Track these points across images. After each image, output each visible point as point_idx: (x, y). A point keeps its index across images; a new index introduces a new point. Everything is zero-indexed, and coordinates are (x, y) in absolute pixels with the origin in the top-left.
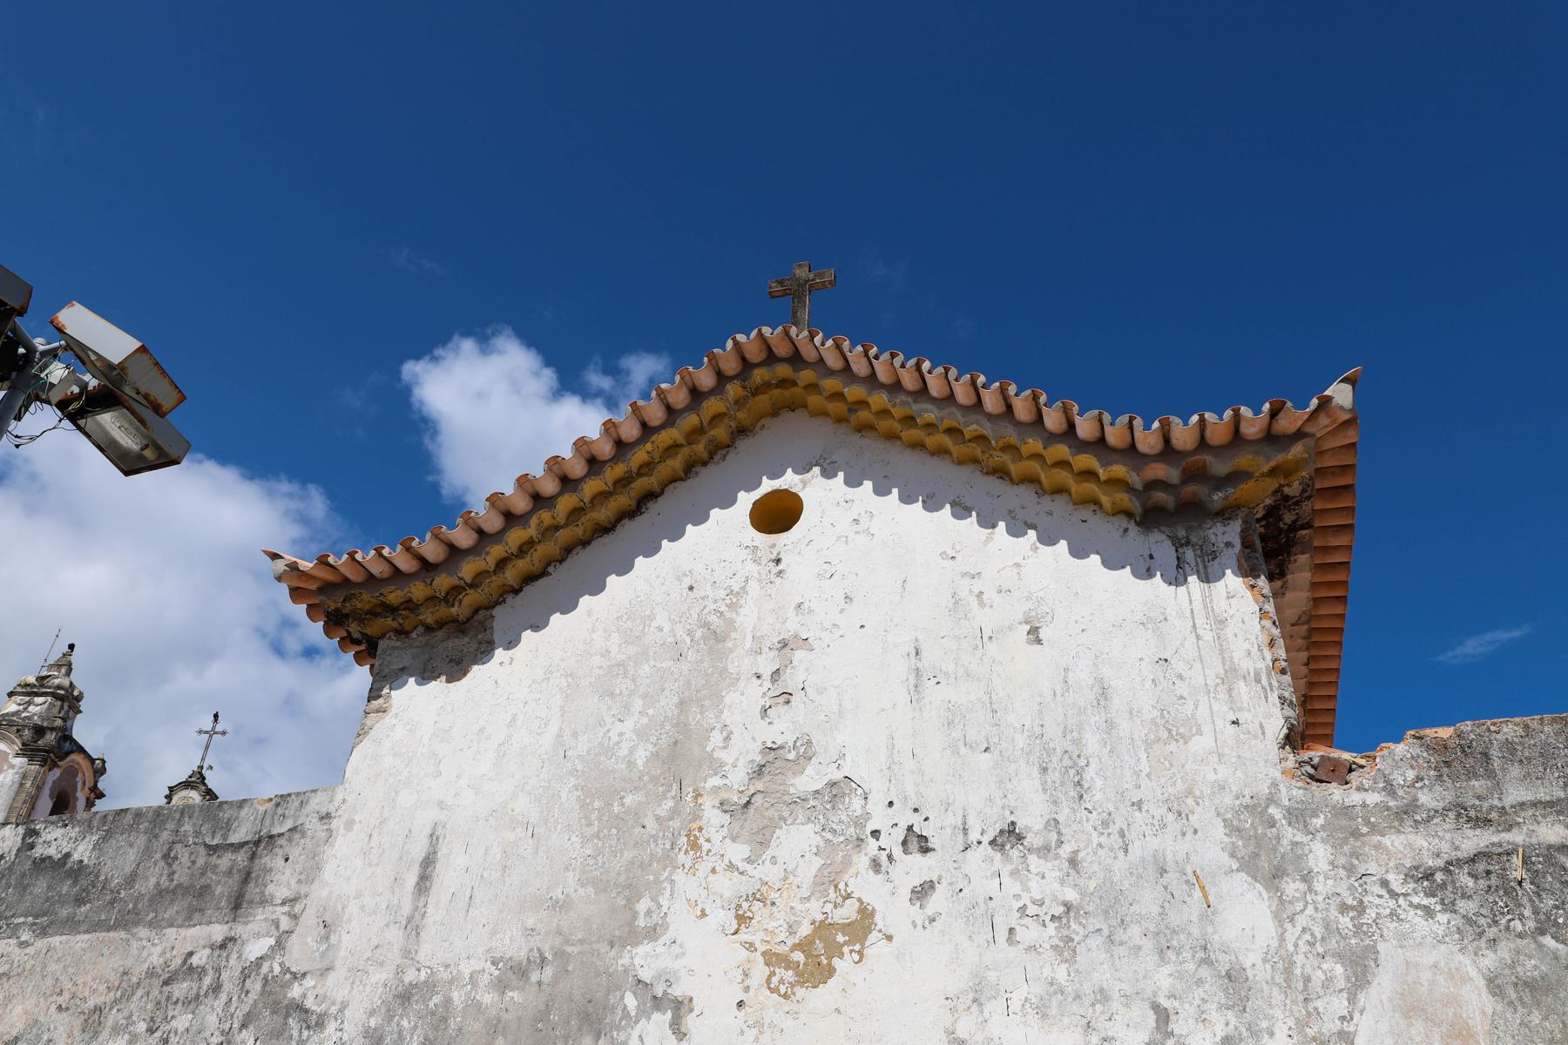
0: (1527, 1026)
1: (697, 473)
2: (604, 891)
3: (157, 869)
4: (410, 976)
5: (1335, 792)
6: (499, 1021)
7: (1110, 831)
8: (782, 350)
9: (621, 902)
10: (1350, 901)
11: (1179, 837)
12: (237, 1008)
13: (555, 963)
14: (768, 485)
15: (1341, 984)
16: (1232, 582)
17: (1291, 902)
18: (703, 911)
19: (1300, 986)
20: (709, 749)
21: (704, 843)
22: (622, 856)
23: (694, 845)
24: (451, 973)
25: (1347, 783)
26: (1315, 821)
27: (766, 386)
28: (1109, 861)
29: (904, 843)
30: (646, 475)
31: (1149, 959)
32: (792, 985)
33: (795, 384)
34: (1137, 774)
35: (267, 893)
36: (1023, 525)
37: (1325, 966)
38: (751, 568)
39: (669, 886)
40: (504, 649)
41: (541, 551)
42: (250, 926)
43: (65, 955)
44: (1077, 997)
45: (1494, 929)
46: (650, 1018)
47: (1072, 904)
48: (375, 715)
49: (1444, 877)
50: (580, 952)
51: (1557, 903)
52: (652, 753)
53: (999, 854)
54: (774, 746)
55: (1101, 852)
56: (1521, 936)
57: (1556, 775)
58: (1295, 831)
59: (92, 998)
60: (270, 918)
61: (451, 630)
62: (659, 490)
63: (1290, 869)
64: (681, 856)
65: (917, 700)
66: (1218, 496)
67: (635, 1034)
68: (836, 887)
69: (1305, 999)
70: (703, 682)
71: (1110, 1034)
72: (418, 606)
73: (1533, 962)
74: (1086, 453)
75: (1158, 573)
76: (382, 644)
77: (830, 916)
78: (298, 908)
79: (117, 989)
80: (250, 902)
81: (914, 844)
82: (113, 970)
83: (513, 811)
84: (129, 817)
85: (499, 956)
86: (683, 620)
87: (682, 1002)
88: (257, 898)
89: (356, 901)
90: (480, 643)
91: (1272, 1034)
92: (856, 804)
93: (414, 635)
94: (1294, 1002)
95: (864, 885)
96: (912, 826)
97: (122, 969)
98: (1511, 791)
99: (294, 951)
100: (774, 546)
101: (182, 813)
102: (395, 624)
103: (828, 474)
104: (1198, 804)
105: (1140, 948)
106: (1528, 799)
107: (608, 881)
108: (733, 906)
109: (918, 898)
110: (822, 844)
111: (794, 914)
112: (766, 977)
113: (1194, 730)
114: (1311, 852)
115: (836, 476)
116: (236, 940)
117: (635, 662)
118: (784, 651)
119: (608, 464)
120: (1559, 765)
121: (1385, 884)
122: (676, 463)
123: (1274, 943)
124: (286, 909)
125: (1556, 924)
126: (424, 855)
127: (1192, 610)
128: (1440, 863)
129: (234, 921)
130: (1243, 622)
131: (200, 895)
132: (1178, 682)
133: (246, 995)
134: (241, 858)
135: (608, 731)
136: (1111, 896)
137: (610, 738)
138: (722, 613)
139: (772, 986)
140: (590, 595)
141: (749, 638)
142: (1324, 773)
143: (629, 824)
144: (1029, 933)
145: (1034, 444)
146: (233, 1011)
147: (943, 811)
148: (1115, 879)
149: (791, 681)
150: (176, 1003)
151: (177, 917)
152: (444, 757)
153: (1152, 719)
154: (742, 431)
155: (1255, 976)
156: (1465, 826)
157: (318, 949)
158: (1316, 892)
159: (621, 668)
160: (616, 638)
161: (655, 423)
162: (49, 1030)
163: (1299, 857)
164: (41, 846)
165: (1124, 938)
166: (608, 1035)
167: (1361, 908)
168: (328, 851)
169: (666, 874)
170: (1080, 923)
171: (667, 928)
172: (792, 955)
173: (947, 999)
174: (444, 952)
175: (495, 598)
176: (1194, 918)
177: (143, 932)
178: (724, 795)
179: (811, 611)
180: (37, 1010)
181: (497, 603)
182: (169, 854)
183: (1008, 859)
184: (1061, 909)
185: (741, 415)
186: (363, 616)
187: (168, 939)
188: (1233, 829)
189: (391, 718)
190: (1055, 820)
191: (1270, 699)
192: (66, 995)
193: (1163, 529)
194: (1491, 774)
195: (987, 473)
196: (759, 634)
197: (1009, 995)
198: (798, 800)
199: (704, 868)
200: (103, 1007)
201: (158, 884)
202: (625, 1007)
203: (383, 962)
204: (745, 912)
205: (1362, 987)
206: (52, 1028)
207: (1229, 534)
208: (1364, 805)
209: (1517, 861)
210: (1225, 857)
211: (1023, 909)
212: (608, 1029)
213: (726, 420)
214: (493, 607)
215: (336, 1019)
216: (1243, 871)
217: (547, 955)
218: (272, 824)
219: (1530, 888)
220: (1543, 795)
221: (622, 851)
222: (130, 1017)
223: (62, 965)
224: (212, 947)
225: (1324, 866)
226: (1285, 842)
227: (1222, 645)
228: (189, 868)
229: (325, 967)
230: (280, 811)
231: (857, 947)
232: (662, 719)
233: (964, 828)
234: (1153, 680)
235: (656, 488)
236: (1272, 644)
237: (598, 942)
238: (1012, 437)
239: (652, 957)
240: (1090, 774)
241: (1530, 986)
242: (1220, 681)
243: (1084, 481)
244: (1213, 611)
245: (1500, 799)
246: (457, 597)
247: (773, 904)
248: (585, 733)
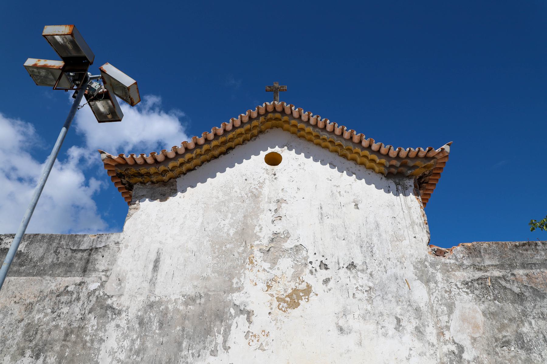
0: (492, 325)
1: (246, 143)
2: (221, 275)
3: (52, 256)
4: (152, 299)
5: (443, 259)
6: (186, 315)
7: (381, 266)
8: (279, 109)
9: (227, 279)
10: (447, 290)
11: (401, 269)
12: (87, 306)
13: (205, 297)
14: (270, 150)
15: (446, 312)
16: (412, 197)
17: (432, 289)
18: (256, 283)
19: (435, 313)
20: (255, 232)
21: (255, 262)
22: (227, 264)
23: (251, 262)
24: (167, 299)
25: (444, 257)
26: (438, 267)
27: (271, 119)
28: (381, 275)
29: (320, 266)
31: (394, 304)
32: (286, 308)
33: (280, 120)
34: (388, 250)
35: (96, 268)
36: (352, 173)
37: (442, 307)
38: (266, 176)
39: (243, 274)
40: (181, 193)
41: (195, 162)
42: (90, 278)
43: (16, 284)
44: (374, 314)
45: (484, 299)
46: (239, 317)
47: (371, 287)
48: (134, 210)
49: (471, 284)
50: (213, 294)
52: (235, 232)
53: (349, 271)
54: (277, 233)
55: (379, 272)
56: (490, 300)
57: (497, 258)
58: (432, 269)
59: (28, 299)
60: (98, 276)
61: (161, 184)
62: (234, 147)
63: (431, 280)
64: (247, 266)
65: (322, 222)
66: (409, 172)
67: (235, 321)
68: (299, 278)
69: (437, 316)
70: (252, 210)
71: (384, 325)
72: (151, 175)
73: (493, 308)
75: (391, 192)
76: (135, 186)
77: (298, 287)
78: (108, 273)
79: (38, 297)
80: (90, 270)
81: (323, 267)
82: (36, 290)
83: (187, 246)
84: (40, 237)
85: (185, 294)
86: (244, 190)
87: (250, 312)
88: (92, 269)
89: (131, 272)
90: (172, 189)
91: (428, 326)
92: (304, 253)
93: (147, 184)
94: (434, 317)
95: (308, 278)
96: (322, 261)
97: (40, 290)
98: (486, 261)
99: (108, 288)
100: (273, 170)
101: (61, 237)
102: (141, 180)
103: (290, 149)
104: (406, 260)
105: (391, 301)
107: (222, 272)
108: (266, 282)
109: (325, 283)
110: (294, 265)
111: (286, 286)
112: (278, 305)
113: (404, 239)
114: (437, 275)
115: (292, 150)
116: (85, 283)
117: (228, 201)
118: (278, 203)
121: (456, 285)
122: (241, 139)
123: (428, 301)
124: (104, 273)
125: (498, 298)
126: (155, 259)
128: (470, 280)
129: (84, 276)
130: (416, 209)
131: (70, 266)
132: (398, 224)
133: (90, 302)
134: (85, 255)
135: (220, 223)
136: (382, 285)
137: (220, 225)
138: (257, 189)
139: (280, 308)
140: (211, 178)
141: (267, 198)
142: (438, 253)
143: (229, 254)
144: (359, 295)
145: (358, 150)
146: (85, 307)
147: (331, 257)
148: (384, 280)
149: (281, 212)
150: (63, 303)
151: (61, 273)
152: (161, 227)
153: (392, 234)
154: (261, 132)
155: (423, 310)
157: (117, 288)
158: (438, 287)
159: (223, 203)
160: (221, 193)
162: (11, 310)
163: (434, 277)
164: (3, 244)
165: (387, 298)
166: (225, 321)
167: (450, 292)
168: (119, 255)
169: (242, 271)
170: (374, 293)
171: (244, 288)
172: (286, 298)
173: (336, 314)
174: (164, 291)
175: (177, 175)
176: (406, 293)
177: (48, 278)
178: (261, 247)
179: (286, 192)
180: (6, 303)
181: (178, 177)
182: (57, 251)
183: (351, 273)
184: (368, 289)
185: (263, 127)
186: (130, 176)
187: (58, 281)
188: (416, 268)
189: (140, 212)
190: (365, 262)
192: (18, 298)
193: (392, 179)
194: (481, 257)
195: (340, 156)
196: (269, 197)
197: (354, 313)
198: (285, 250)
199: (255, 270)
200: (33, 303)
201: (52, 261)
202: (231, 313)
203: (142, 293)
204: (270, 285)
205: (451, 313)
206: (12, 309)
207: (410, 183)
208: (450, 263)
209: (488, 280)
210: (414, 276)
211: (357, 288)
212: (225, 320)
213: (258, 128)
214: (176, 178)
215: (125, 312)
216: (419, 280)
217: (202, 294)
218: (97, 244)
220: (494, 263)
221: (226, 263)
222: (44, 307)
223: (15, 287)
224: (76, 285)
225: (440, 280)
226: (430, 272)
227: (410, 215)
228: (65, 257)
229: (120, 294)
230: (99, 240)
231: (307, 297)
232: (238, 221)
233: (338, 263)
234: (392, 223)
235: (233, 146)
236: (423, 216)
237: (220, 291)
238: (351, 147)
239: (239, 297)
240: (375, 249)
241: (492, 314)
242: (410, 225)
243: (371, 162)
244: (407, 204)
245: (484, 263)
246: (165, 173)
247: (279, 282)
248: (211, 223)
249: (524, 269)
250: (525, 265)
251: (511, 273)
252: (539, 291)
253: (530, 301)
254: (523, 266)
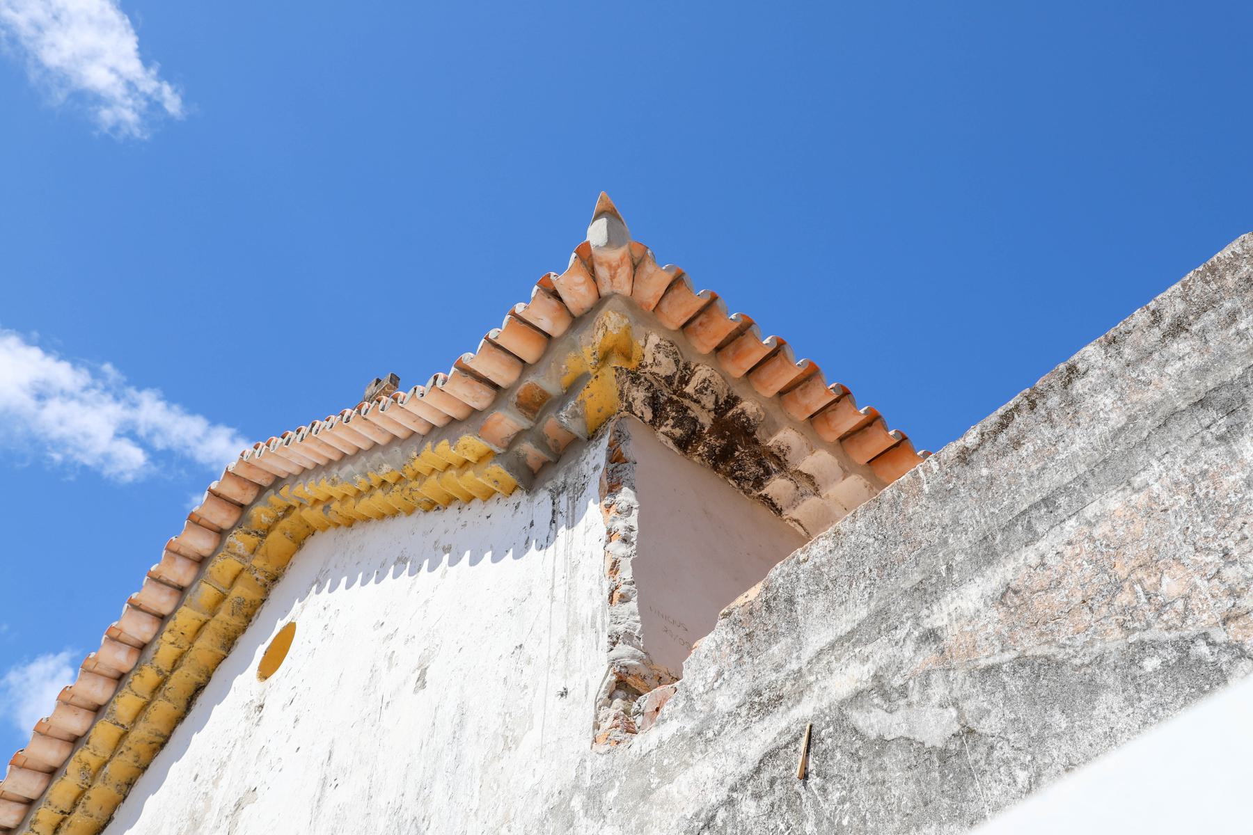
30: (179, 667)
41: (100, 794)
51: (844, 793)
57: (862, 586)
74: (442, 440)
106: (828, 640)
119: (133, 673)
120: (867, 571)
122: (206, 645)
127: (554, 568)
128: (723, 793)
156: (754, 719)
161: (166, 610)
191: (600, 645)
194: (793, 624)
219: (815, 784)
220: (844, 627)
236: (614, 568)
249: (990, 563)
250: (999, 537)
251: (916, 633)
252: (1060, 665)
253: (1006, 762)
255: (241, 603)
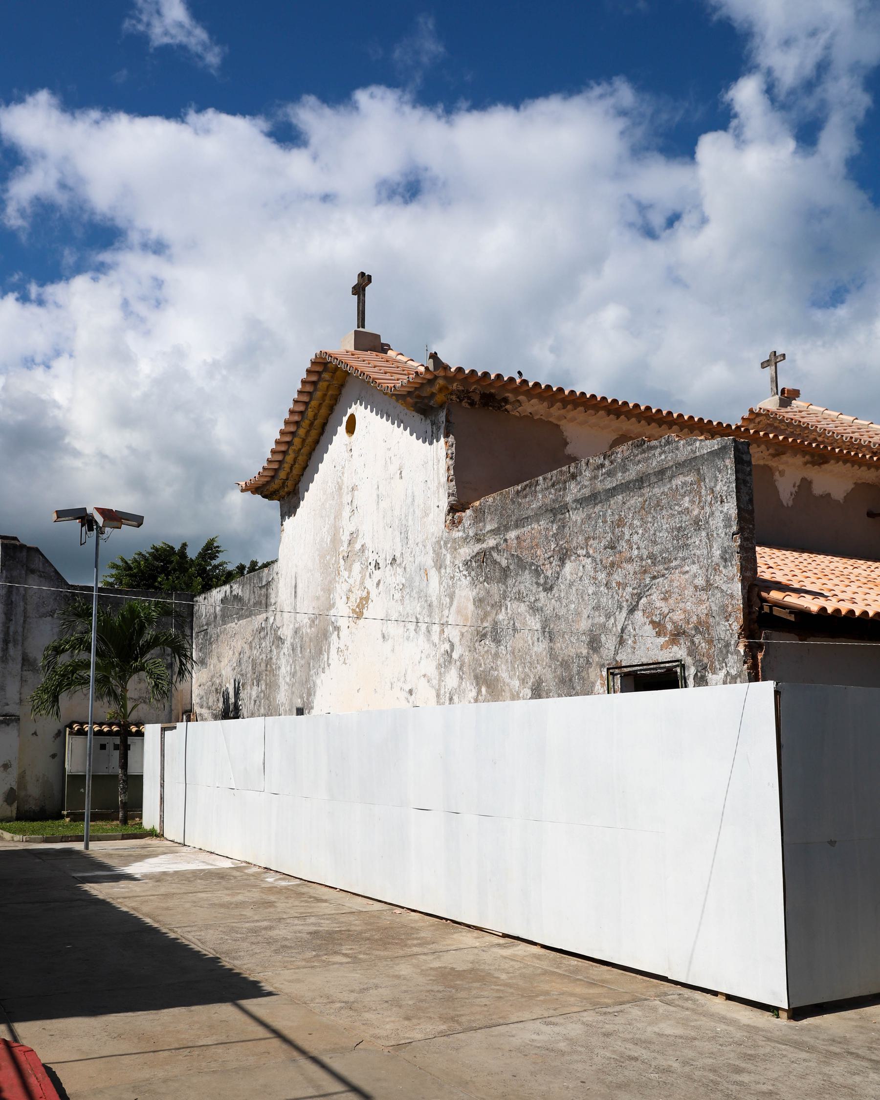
30: (317, 419)
122: (323, 411)
161: (307, 401)
236: (448, 469)
254: (517, 526)
255: (332, 395)
